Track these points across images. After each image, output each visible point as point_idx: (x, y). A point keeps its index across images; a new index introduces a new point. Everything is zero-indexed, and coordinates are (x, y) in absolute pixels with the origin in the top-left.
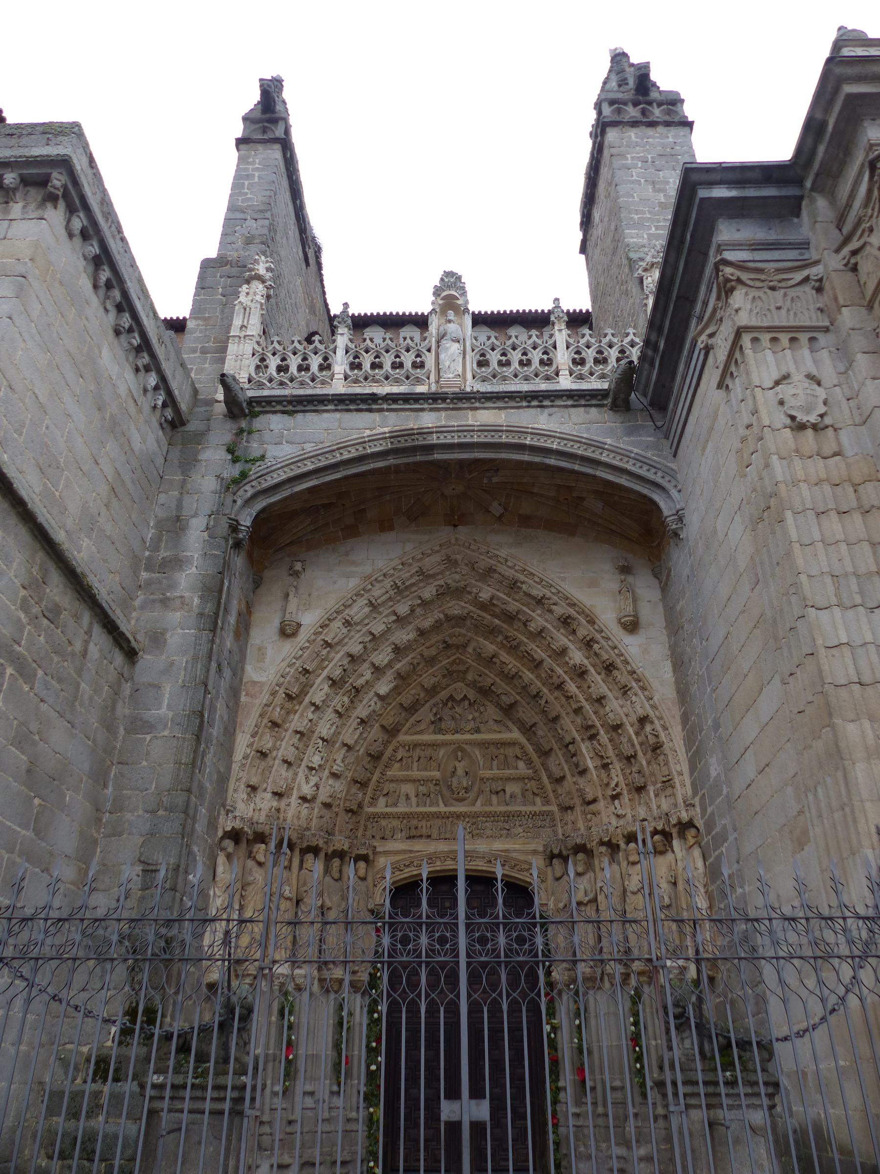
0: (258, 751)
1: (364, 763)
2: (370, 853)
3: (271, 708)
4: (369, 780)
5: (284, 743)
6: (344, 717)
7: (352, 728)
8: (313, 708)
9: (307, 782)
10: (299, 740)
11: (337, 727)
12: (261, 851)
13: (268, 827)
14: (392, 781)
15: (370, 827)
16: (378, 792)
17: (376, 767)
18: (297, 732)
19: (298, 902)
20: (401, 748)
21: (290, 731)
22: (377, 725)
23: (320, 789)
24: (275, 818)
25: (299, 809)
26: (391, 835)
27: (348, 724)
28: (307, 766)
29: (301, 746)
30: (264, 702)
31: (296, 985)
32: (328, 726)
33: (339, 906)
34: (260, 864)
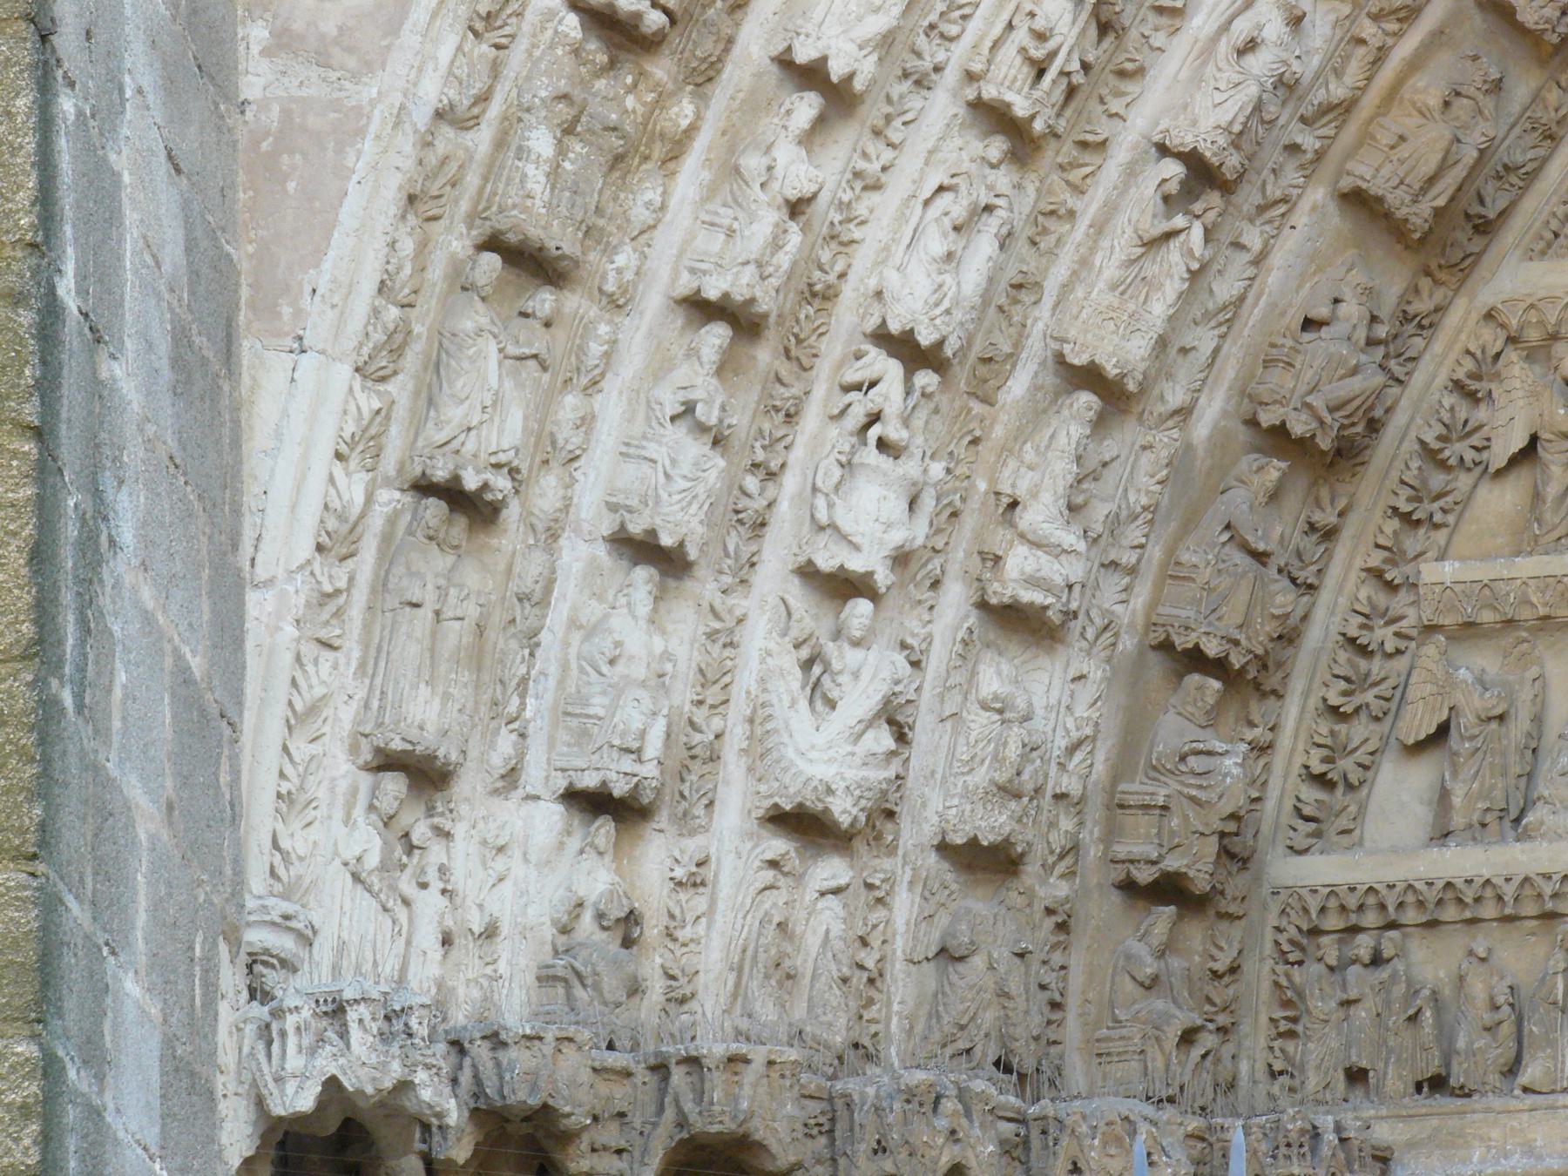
0: (424, 488)
1: (1239, 502)
3: (481, 139)
4: (1288, 637)
5: (611, 405)
6: (1050, 155)
7: (1120, 244)
8: (806, 107)
9: (820, 696)
10: (726, 367)
11: (1005, 242)
13: (573, 1065)
14: (1470, 629)
15: (1321, 1004)
16: (1359, 730)
17: (1329, 534)
18: (701, 309)
20: (1516, 369)
21: (653, 302)
22: (1318, 194)
23: (925, 732)
26: (1501, 1052)
27: (1089, 208)
28: (808, 573)
29: (739, 420)
30: (432, 91)
32: (935, 244)
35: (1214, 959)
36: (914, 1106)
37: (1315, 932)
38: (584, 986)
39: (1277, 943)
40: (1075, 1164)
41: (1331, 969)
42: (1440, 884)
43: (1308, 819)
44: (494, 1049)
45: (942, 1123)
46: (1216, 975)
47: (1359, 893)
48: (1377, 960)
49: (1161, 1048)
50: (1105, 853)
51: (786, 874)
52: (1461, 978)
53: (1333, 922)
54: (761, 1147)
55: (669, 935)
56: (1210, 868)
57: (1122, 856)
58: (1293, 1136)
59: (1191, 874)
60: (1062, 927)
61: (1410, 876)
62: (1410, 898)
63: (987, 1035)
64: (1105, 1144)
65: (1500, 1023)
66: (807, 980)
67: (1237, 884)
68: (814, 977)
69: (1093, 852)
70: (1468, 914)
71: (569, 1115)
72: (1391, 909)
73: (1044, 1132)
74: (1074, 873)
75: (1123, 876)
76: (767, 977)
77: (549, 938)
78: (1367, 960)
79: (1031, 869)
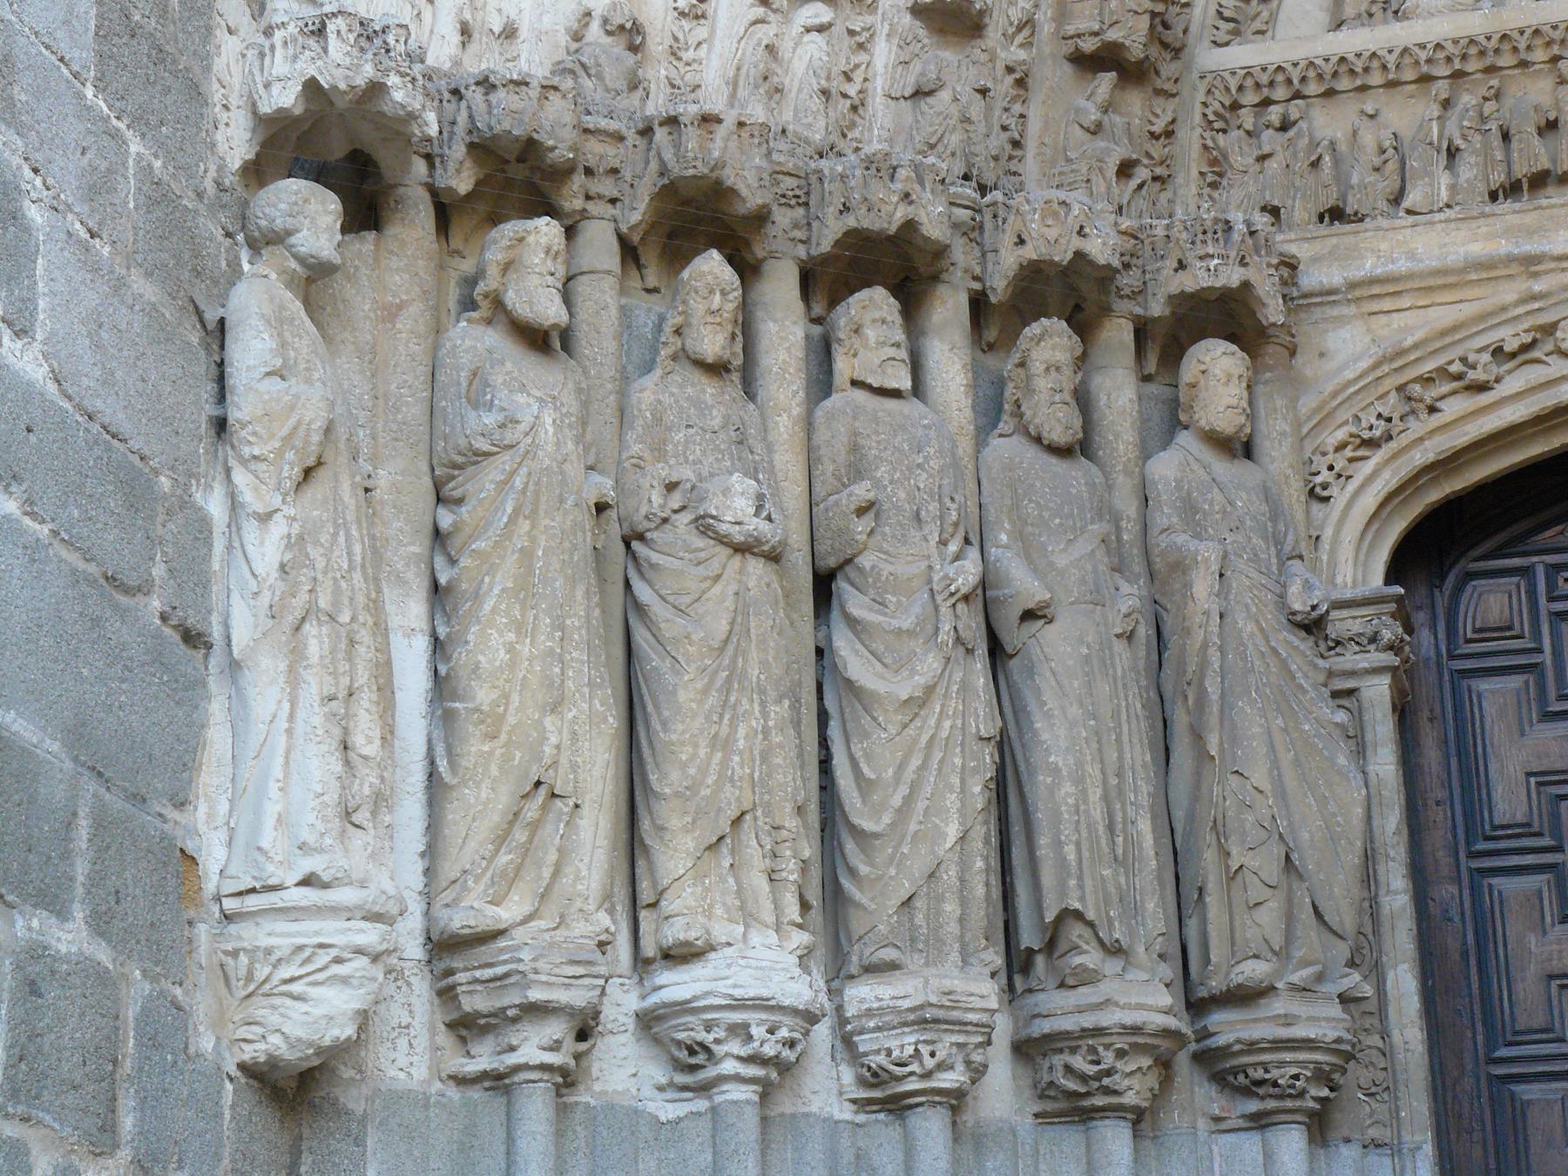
2: (1267, 287)
12: (537, 259)
15: (1240, 154)
19: (824, 586)
24: (613, 76)
25: (765, 33)
26: (1389, 184)
31: (875, 1078)
33: (1097, 600)
34: (537, 339)
35: (1152, 124)
36: (873, 171)
37: (1235, 106)
38: (589, 76)
39: (1205, 115)
40: (1019, 236)
41: (1248, 133)
42: (1334, 59)
43: (1228, 20)
44: (486, 94)
45: (898, 186)
46: (1154, 136)
47: (1269, 72)
48: (1285, 126)
49: (1104, 178)
50: (1058, 30)
51: (775, 11)
52: (1355, 133)
53: (1250, 98)
54: (732, 192)
55: (673, 54)
56: (1143, 40)
57: (1071, 33)
58: (1209, 223)
59: (1127, 43)
60: (1020, 83)
61: (1310, 54)
62: (1311, 74)
63: (953, 154)
64: (1043, 218)
65: (1385, 162)
66: (793, 94)
67: (1168, 69)
68: (800, 90)
69: (1046, 28)
70: (1359, 82)
71: (553, 149)
72: (1296, 81)
73: (995, 216)
74: (1031, 44)
75: (1072, 49)
76: (756, 87)
77: (563, 44)
78: (1278, 125)
79: (993, 34)
